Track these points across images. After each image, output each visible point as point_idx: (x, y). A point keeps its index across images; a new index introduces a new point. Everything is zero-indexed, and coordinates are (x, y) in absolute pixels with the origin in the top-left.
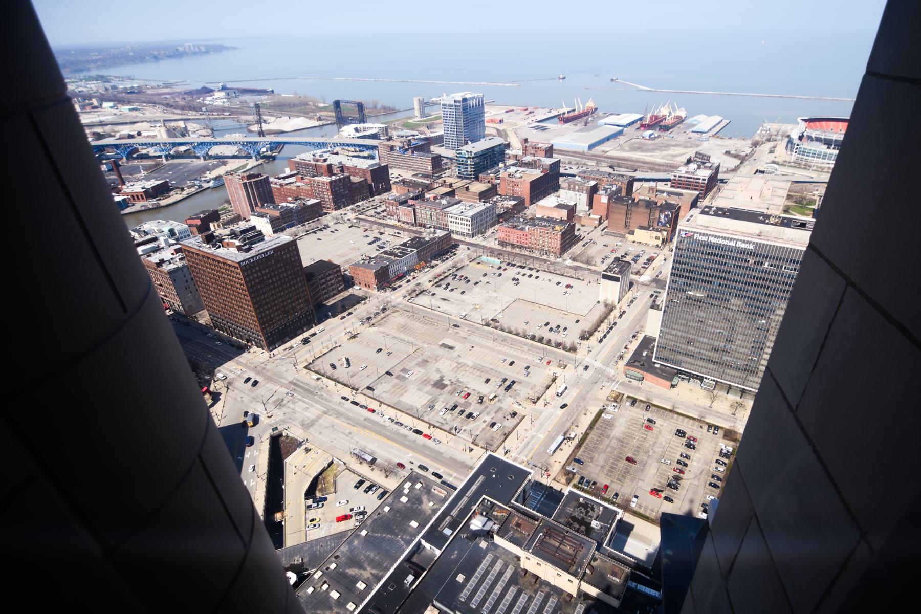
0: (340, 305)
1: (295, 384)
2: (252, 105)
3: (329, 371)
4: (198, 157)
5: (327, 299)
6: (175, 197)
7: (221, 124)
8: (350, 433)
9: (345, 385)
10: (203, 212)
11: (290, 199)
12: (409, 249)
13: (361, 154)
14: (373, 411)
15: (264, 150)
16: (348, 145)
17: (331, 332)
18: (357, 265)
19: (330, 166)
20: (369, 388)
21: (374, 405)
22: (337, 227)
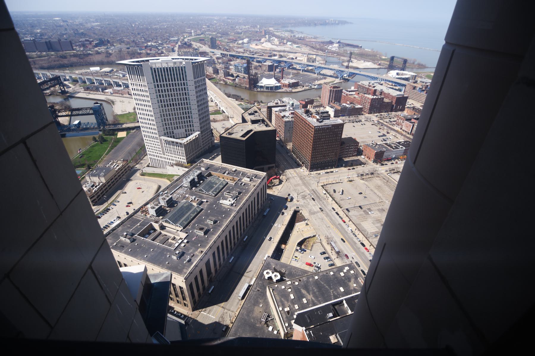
0: (351, 162)
1: (314, 192)
2: (349, 52)
3: (332, 192)
4: (315, 73)
5: (346, 157)
6: (299, 89)
7: (331, 59)
8: (329, 227)
9: (336, 202)
10: (307, 99)
11: (348, 102)
12: (401, 146)
13: (394, 87)
14: (345, 222)
15: (345, 75)
16: (389, 81)
17: (342, 174)
18: (368, 145)
19: (375, 91)
20: (347, 210)
21: (346, 219)
22: (365, 123)
